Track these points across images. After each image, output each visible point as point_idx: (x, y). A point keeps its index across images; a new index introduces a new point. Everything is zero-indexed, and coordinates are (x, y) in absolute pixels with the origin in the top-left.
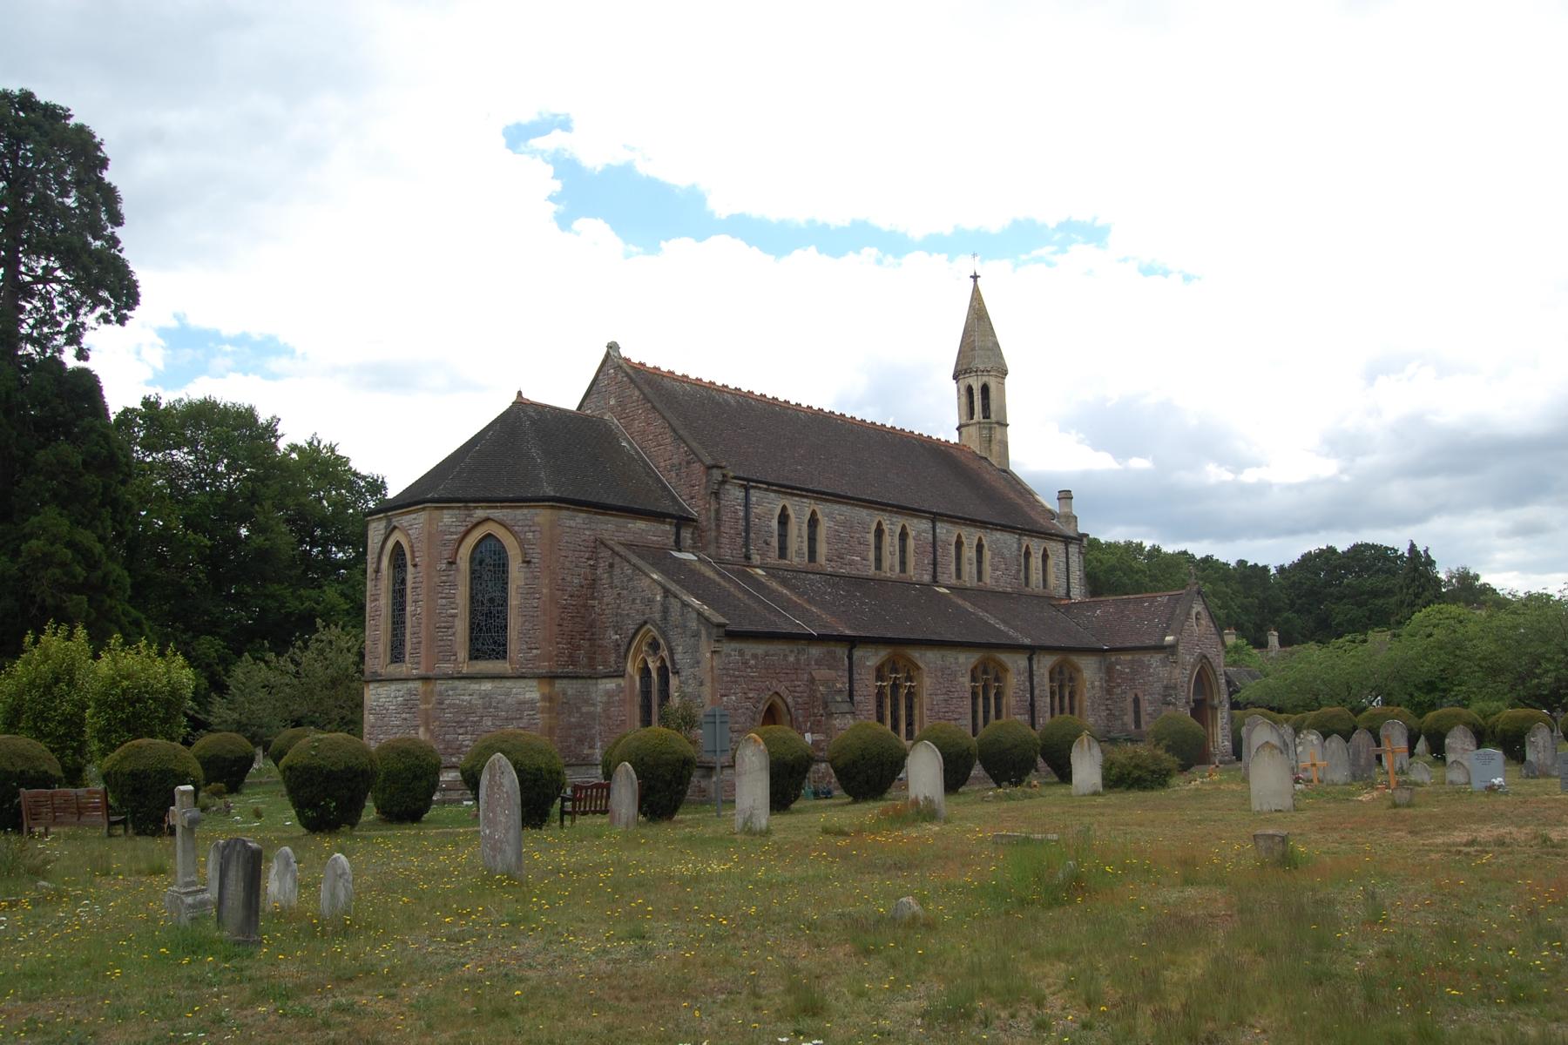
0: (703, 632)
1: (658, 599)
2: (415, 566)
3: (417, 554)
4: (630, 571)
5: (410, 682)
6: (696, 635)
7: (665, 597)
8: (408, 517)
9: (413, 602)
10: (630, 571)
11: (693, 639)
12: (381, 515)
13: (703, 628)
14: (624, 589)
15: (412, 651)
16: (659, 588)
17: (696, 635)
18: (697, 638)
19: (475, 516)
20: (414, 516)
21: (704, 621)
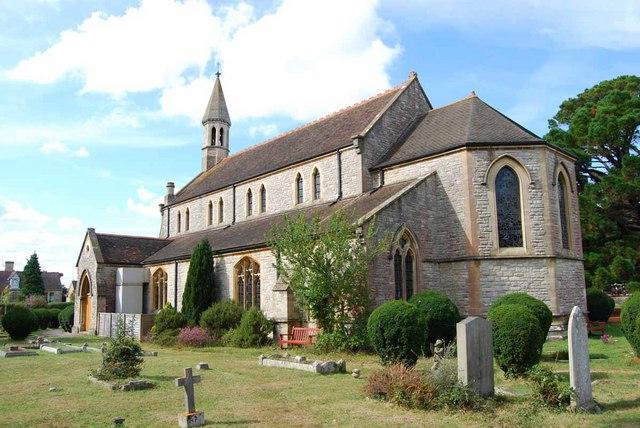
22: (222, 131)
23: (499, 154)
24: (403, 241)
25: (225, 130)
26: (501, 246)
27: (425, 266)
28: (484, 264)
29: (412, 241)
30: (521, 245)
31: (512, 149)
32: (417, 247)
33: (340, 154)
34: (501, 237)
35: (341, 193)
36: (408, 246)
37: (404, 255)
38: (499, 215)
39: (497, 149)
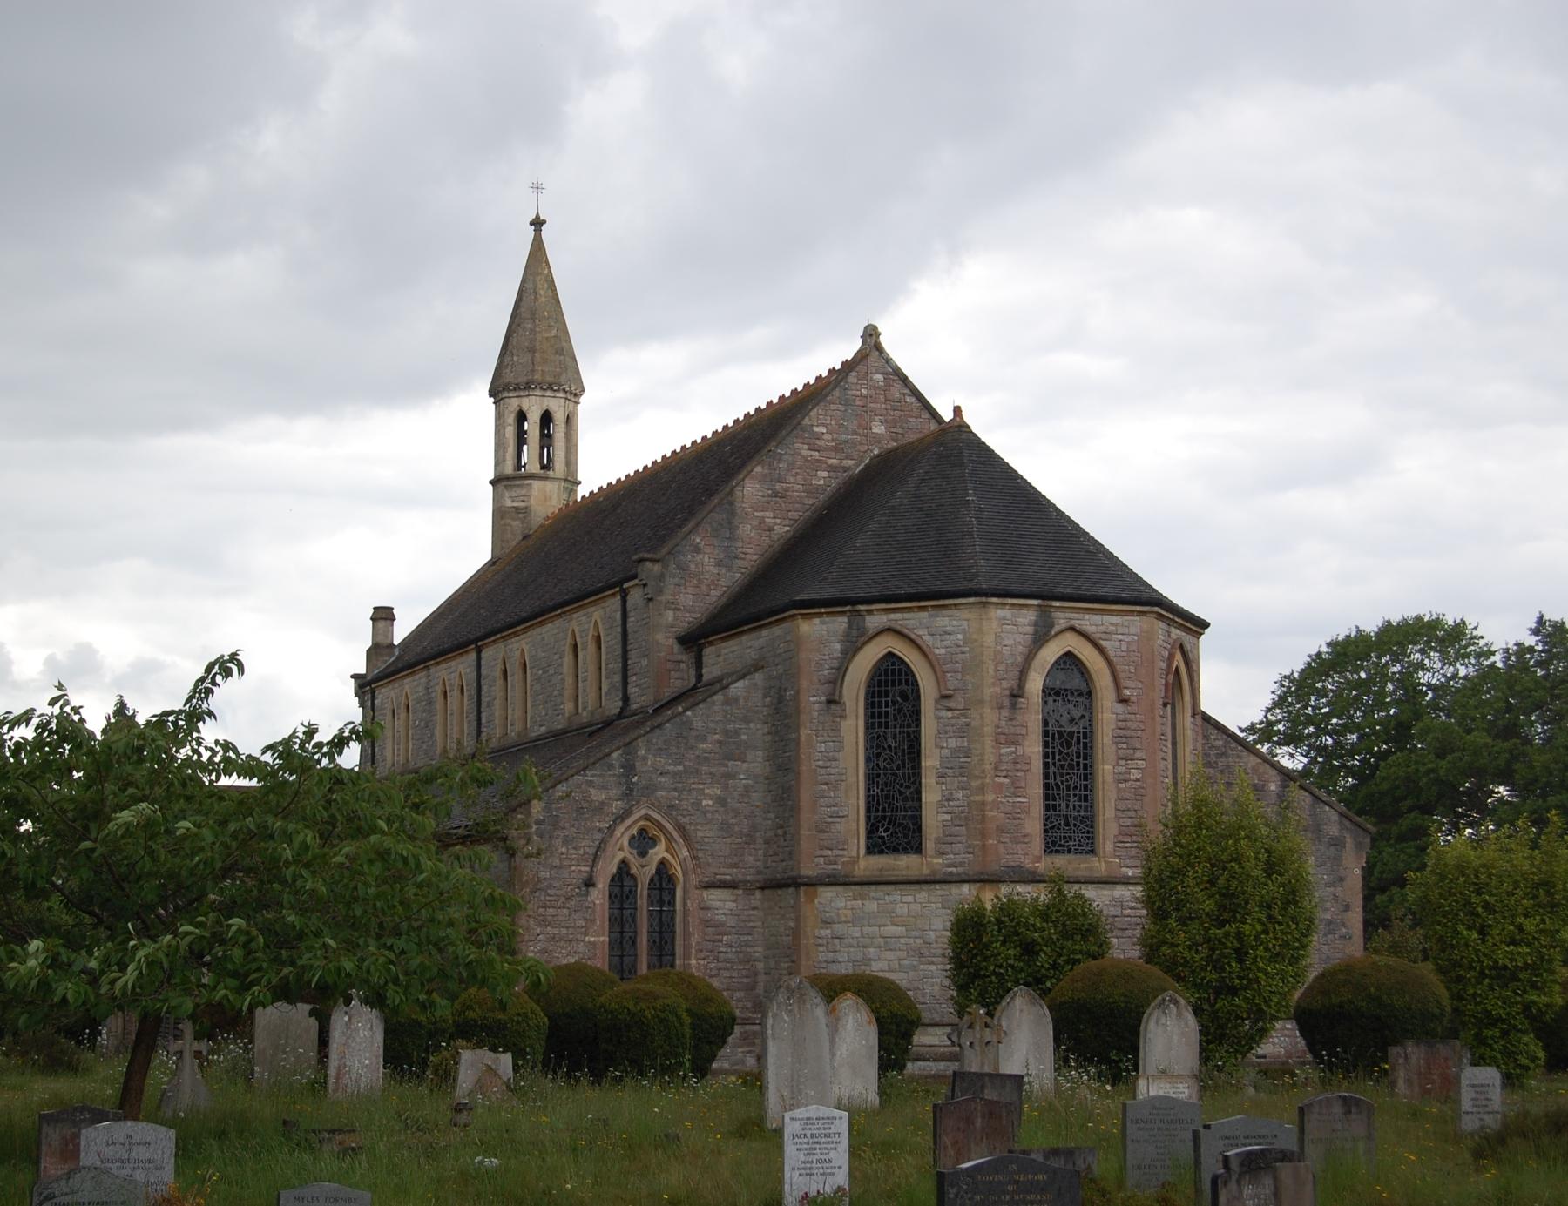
0: (1349, 841)
1: (1273, 787)
2: (1123, 701)
3: (1124, 683)
4: (1221, 743)
5: (1119, 887)
6: (1337, 843)
7: (1284, 786)
8: (1097, 618)
9: (1122, 759)
10: (1221, 743)
11: (1332, 848)
12: (1035, 602)
13: (1348, 836)
14: (1211, 767)
15: (1120, 838)
16: (1275, 772)
17: (1337, 843)
18: (1338, 847)
19: (1172, 635)
20: (1115, 619)
21: (1347, 823)
22: (546, 418)
23: (875, 621)
24: (643, 842)
25: (559, 417)
26: (870, 850)
27: (715, 897)
28: (827, 894)
29: (670, 839)
30: (918, 850)
31: (909, 609)
32: (684, 853)
33: (624, 595)
34: (870, 833)
35: (626, 699)
36: (659, 852)
37: (644, 872)
38: (870, 779)
39: (870, 612)
